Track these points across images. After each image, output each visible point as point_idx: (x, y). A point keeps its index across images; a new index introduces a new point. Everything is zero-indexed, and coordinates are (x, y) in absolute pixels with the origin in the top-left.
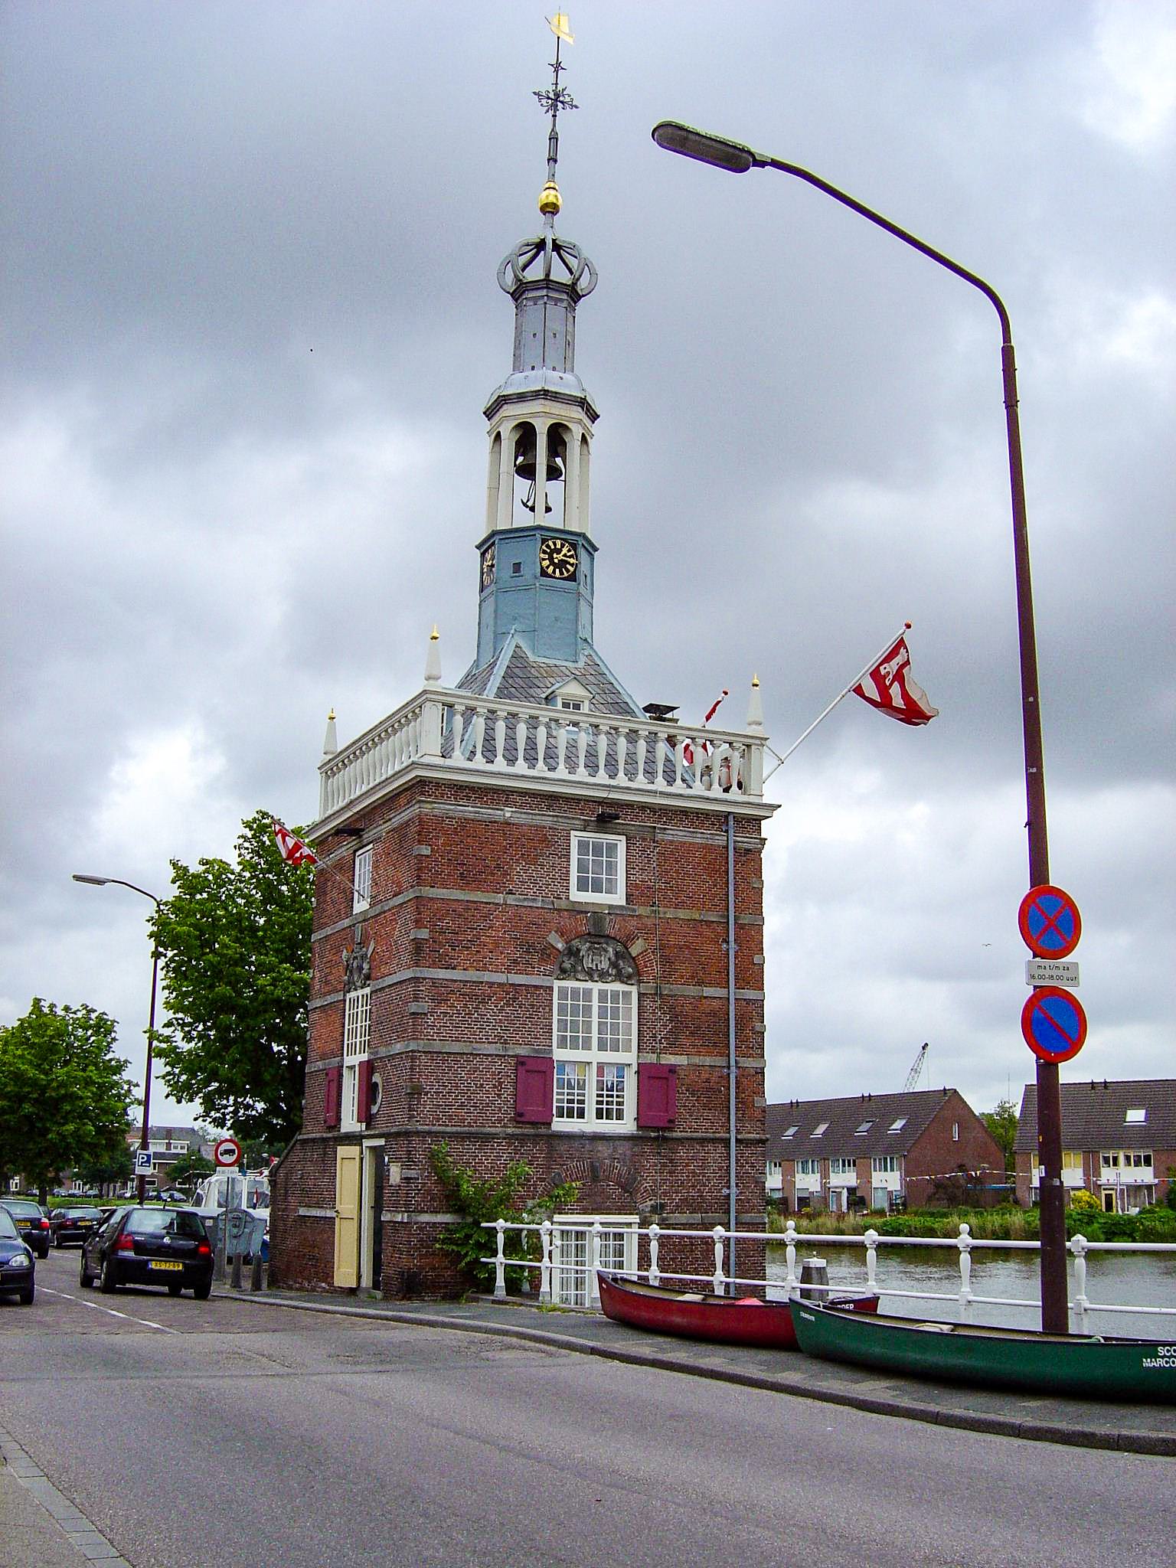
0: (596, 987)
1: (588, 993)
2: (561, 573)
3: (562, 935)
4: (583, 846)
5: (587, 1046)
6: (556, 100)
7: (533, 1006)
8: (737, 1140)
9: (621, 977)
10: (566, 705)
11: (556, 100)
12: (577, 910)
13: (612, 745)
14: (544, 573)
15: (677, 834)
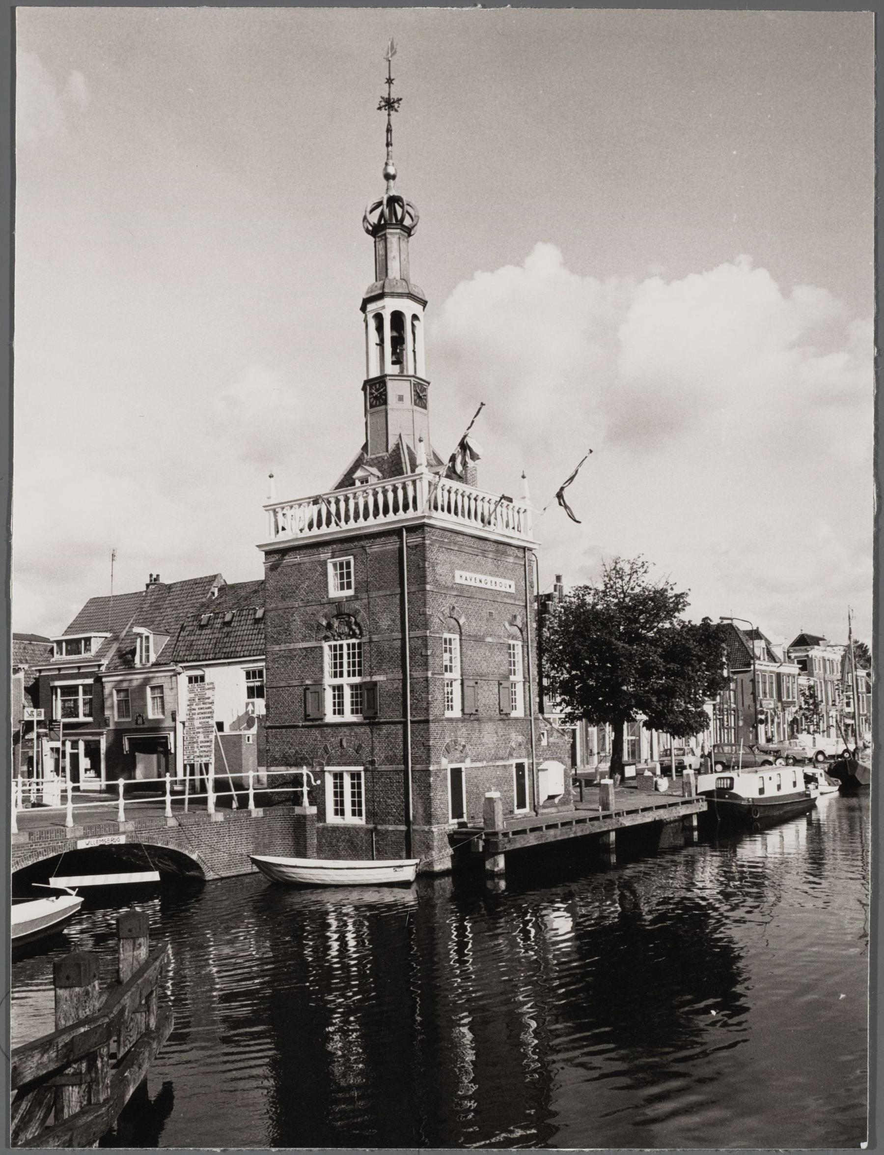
0: (344, 643)
1: (341, 646)
2: (380, 402)
3: (326, 618)
4: (335, 565)
5: (341, 675)
6: (389, 104)
7: (313, 658)
8: (412, 722)
9: (354, 636)
10: (362, 483)
11: (389, 104)
12: (331, 602)
13: (385, 497)
14: (372, 406)
15: (375, 548)
